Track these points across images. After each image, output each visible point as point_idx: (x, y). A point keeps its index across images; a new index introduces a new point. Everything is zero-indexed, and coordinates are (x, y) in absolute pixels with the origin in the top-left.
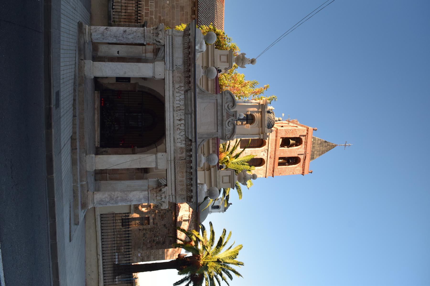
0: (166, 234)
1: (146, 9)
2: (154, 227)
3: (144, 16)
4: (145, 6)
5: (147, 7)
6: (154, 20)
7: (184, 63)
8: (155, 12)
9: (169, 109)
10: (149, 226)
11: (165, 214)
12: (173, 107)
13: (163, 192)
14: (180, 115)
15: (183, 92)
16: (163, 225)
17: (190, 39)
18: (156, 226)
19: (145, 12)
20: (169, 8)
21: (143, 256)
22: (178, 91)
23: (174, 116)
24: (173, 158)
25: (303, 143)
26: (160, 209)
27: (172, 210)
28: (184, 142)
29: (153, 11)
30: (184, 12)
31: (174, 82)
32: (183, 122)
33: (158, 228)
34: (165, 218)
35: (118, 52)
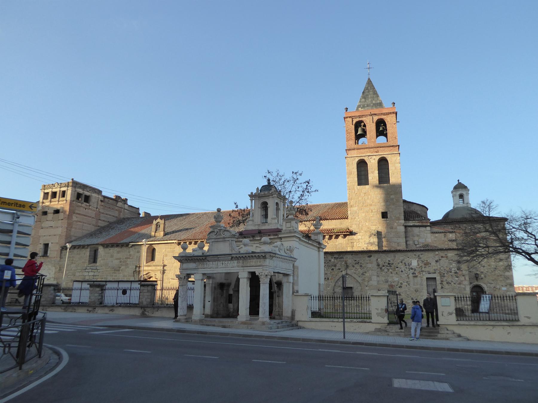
0: (447, 260)
2: (439, 273)
7: (195, 262)
9: (217, 271)
10: (438, 278)
11: (423, 262)
12: (216, 268)
13: (259, 274)
14: (220, 263)
15: (209, 262)
16: (437, 263)
17: (183, 260)
18: (438, 271)
21: (506, 284)
22: (208, 266)
23: (221, 268)
24: (242, 268)
25: (361, 119)
26: (418, 267)
27: (419, 254)
28: (234, 261)
31: (204, 268)
32: (224, 262)
33: (440, 268)
34: (428, 261)
35: (209, 301)
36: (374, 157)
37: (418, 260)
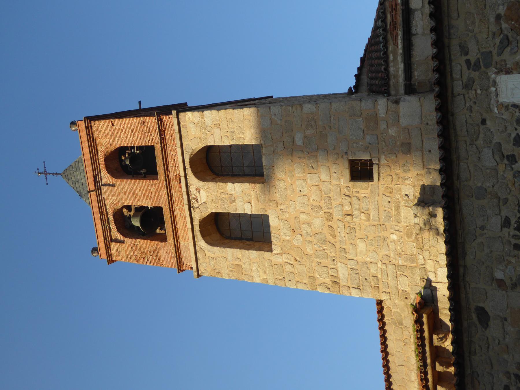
27: (465, 67)
34: (502, 10)
36: (192, 190)
37: (499, 72)
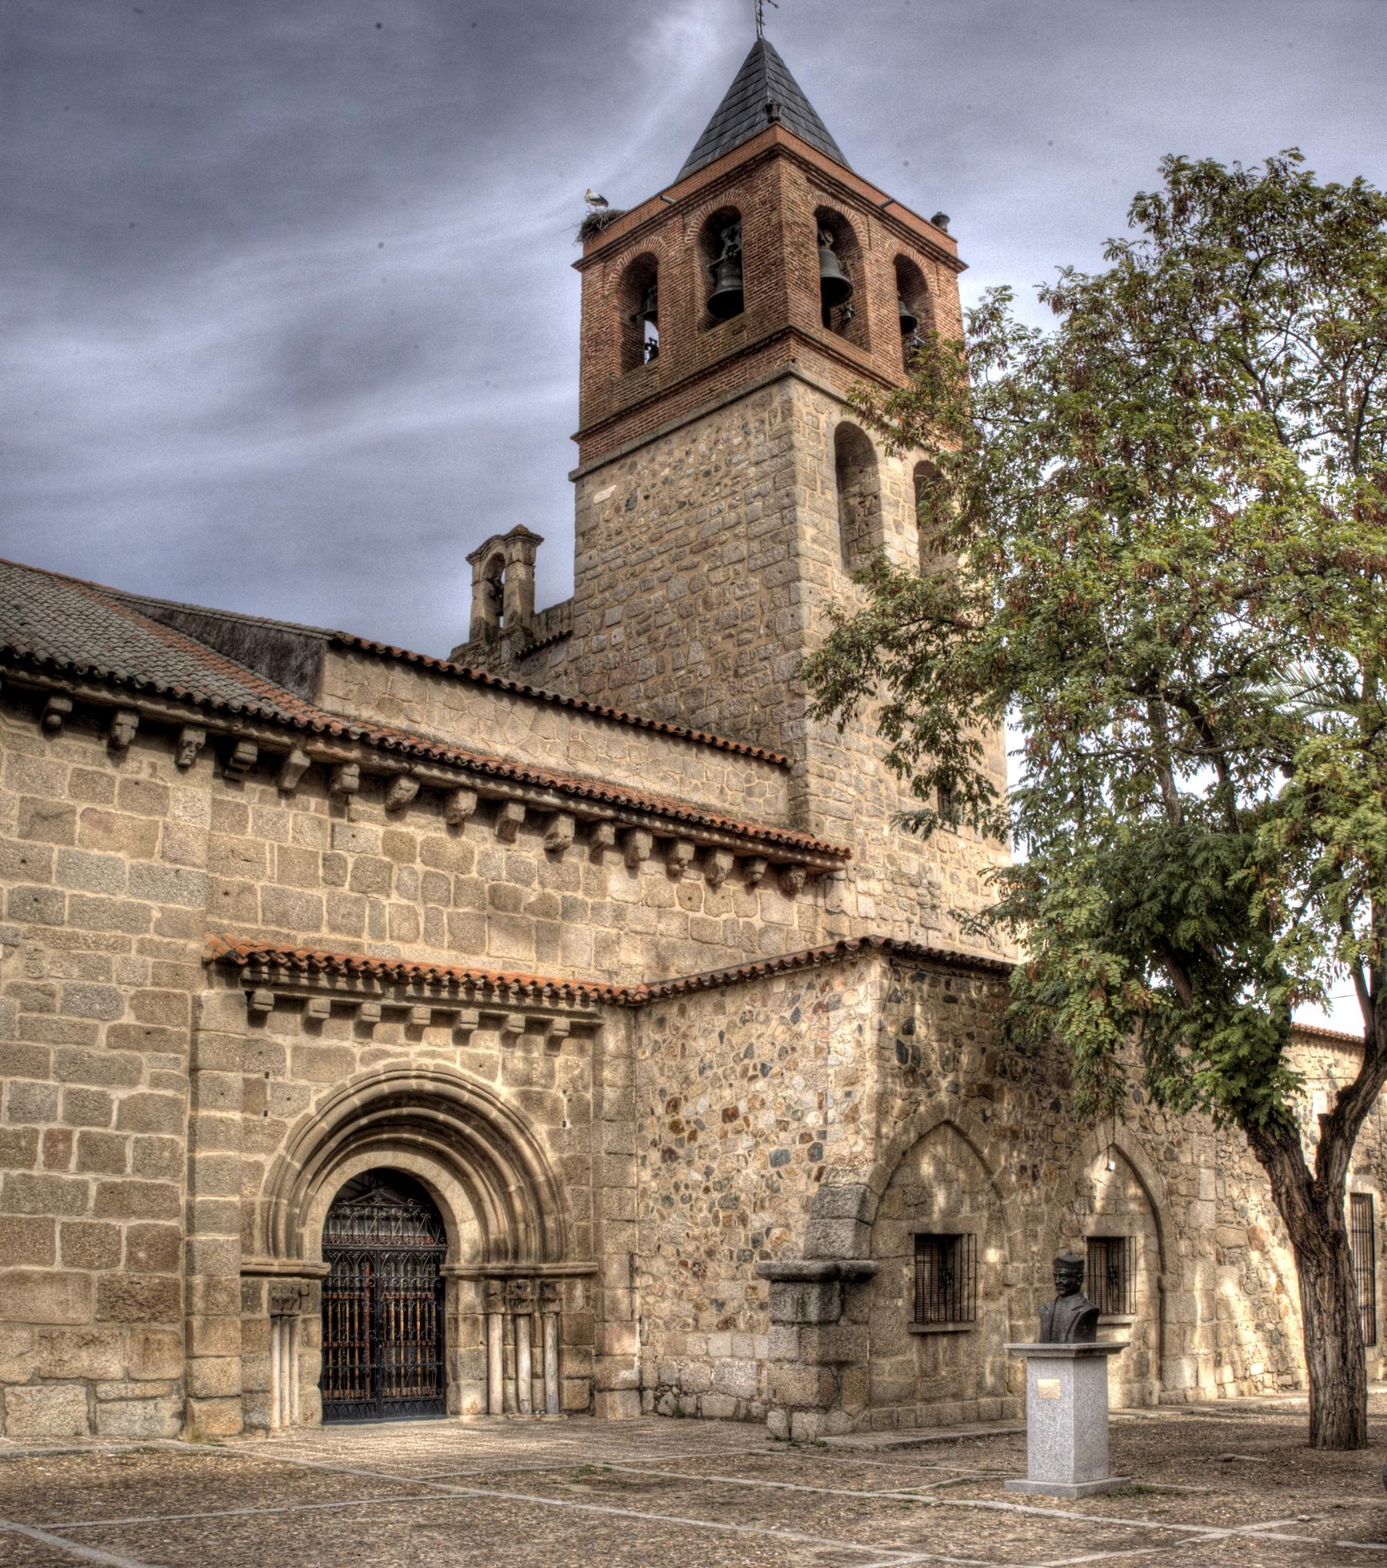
1: (55, 1160)
3: (118, 1179)
4: (30, 1167)
5: (40, 1147)
6: (143, 1089)
8: (80, 1080)
19: (83, 1167)
20: (41, 945)
29: (70, 1093)
30: (79, 810)
